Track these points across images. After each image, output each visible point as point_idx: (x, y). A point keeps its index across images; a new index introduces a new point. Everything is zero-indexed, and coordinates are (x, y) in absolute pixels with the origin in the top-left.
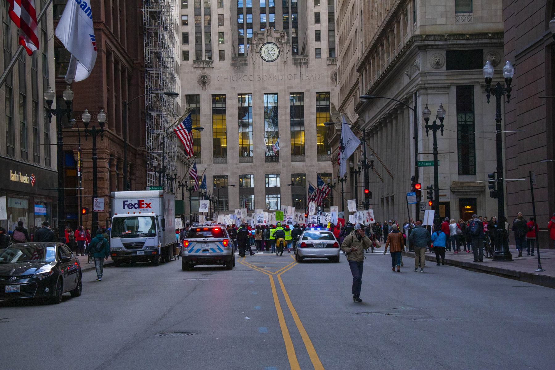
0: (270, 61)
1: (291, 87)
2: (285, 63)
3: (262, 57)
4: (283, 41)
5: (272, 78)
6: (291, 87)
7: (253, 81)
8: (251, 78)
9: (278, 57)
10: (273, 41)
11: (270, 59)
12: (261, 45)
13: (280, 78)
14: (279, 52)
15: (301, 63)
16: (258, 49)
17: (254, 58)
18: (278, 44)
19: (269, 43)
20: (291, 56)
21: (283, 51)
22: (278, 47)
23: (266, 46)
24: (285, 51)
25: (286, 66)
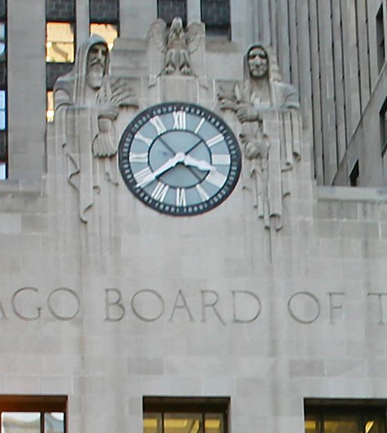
0: (181, 212)
1: (313, 368)
2: (273, 223)
3: (131, 184)
4: (258, 103)
5: (194, 302)
6: (313, 368)
7: (77, 320)
8: (66, 304)
9: (230, 187)
10: (201, 101)
11: (181, 199)
12: (126, 118)
13: (247, 308)
14: (236, 161)
15: (368, 233)
16: (111, 142)
17: (86, 181)
18: (229, 118)
19: (178, 106)
20: (310, 183)
21: (258, 156)
22: (227, 132)
23: (157, 124)
24: (275, 157)
25: (279, 241)
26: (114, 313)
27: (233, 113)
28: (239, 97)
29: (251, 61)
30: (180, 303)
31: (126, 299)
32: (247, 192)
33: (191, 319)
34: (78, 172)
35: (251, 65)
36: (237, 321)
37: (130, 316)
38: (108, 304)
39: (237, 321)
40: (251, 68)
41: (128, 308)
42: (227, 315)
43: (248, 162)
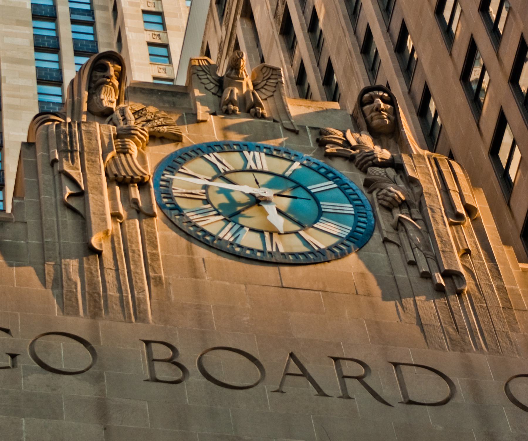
26: (164, 372)
27: (347, 162)
28: (354, 143)
29: (366, 108)
30: (294, 369)
31: (188, 357)
32: (391, 248)
33: (321, 392)
34: (81, 194)
35: (367, 113)
36: (411, 402)
37: (195, 377)
38: (152, 360)
39: (411, 402)
40: (369, 117)
41: (193, 368)
42: (389, 390)
43: (386, 213)
